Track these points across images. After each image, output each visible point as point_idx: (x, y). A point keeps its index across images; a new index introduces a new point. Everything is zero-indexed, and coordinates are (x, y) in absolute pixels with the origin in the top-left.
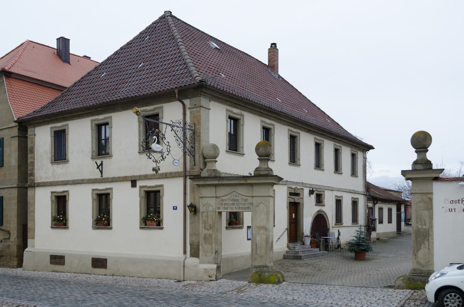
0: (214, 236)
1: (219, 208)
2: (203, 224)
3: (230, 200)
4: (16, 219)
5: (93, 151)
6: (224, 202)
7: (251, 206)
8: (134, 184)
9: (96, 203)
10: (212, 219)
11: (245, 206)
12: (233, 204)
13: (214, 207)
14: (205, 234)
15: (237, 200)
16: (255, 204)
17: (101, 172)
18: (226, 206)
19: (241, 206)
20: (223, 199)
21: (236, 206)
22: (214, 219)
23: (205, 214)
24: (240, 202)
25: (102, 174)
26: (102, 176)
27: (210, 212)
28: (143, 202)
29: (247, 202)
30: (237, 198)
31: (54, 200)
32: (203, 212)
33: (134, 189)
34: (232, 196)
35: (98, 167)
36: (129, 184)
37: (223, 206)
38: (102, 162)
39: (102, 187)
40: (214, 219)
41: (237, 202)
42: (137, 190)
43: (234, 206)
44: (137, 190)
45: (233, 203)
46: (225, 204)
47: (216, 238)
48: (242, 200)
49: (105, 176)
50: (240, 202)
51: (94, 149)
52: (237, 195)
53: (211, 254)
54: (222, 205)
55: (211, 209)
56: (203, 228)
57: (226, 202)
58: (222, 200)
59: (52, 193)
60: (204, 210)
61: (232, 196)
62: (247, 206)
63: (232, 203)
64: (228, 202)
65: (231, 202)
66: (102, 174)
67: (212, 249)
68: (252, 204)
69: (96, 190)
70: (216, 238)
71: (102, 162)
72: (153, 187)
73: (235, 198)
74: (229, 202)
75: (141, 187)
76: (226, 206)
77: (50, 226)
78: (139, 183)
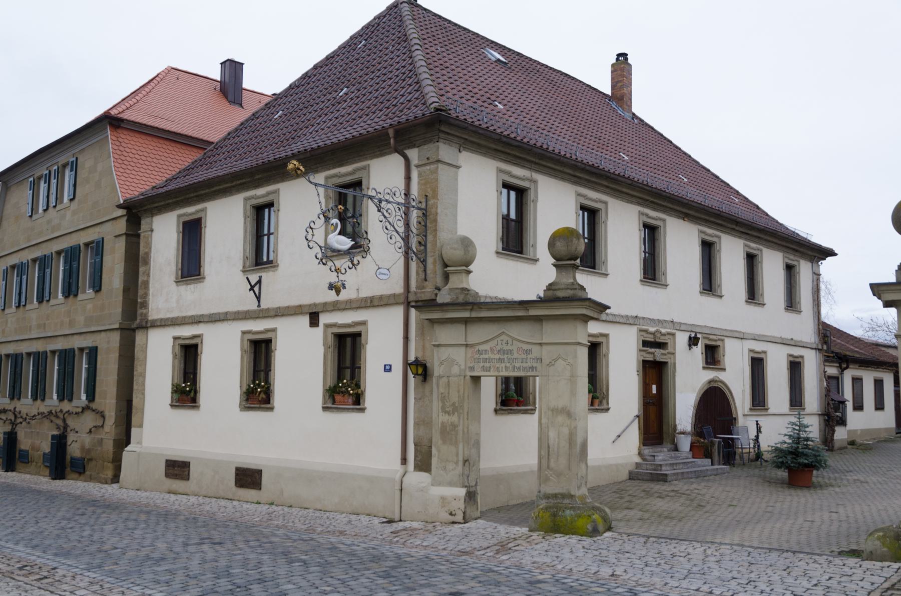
0: (460, 428)
1: (472, 369)
2: (440, 402)
3: (495, 352)
4: (115, 389)
5: (246, 258)
6: (482, 357)
7: (538, 365)
8: (314, 320)
9: (249, 359)
10: (459, 392)
11: (525, 365)
12: (501, 360)
13: (463, 367)
14: (443, 423)
15: (510, 352)
16: (546, 360)
17: (258, 298)
18: (487, 365)
19: (517, 365)
20: (480, 349)
21: (508, 365)
22: (462, 391)
23: (445, 380)
24: (515, 355)
25: (259, 301)
26: (259, 306)
27: (455, 376)
28: (329, 357)
29: (529, 356)
30: (509, 347)
31: (177, 354)
32: (440, 377)
33: (315, 329)
34: (500, 342)
35: (252, 288)
36: (306, 319)
37: (481, 365)
38: (260, 277)
39: (258, 326)
40: (462, 391)
41: (510, 356)
42: (319, 331)
43: (503, 365)
44: (319, 331)
45: (502, 357)
46: (485, 360)
47: (466, 430)
48: (520, 353)
49: (264, 305)
50: (515, 355)
51: (247, 254)
52: (510, 343)
53: (454, 465)
54: (479, 362)
55: (455, 370)
56: (440, 411)
57: (486, 356)
58: (479, 350)
59: (175, 338)
60: (441, 373)
61: (500, 342)
62: (529, 364)
63: (500, 359)
64: (490, 355)
65: (497, 356)
66: (259, 301)
67: (457, 455)
68: (541, 359)
69: (249, 332)
70: (466, 430)
71: (260, 277)
72: (349, 326)
73: (506, 348)
74: (492, 356)
75: (327, 326)
76: (487, 365)
77: (169, 402)
78: (324, 319)
